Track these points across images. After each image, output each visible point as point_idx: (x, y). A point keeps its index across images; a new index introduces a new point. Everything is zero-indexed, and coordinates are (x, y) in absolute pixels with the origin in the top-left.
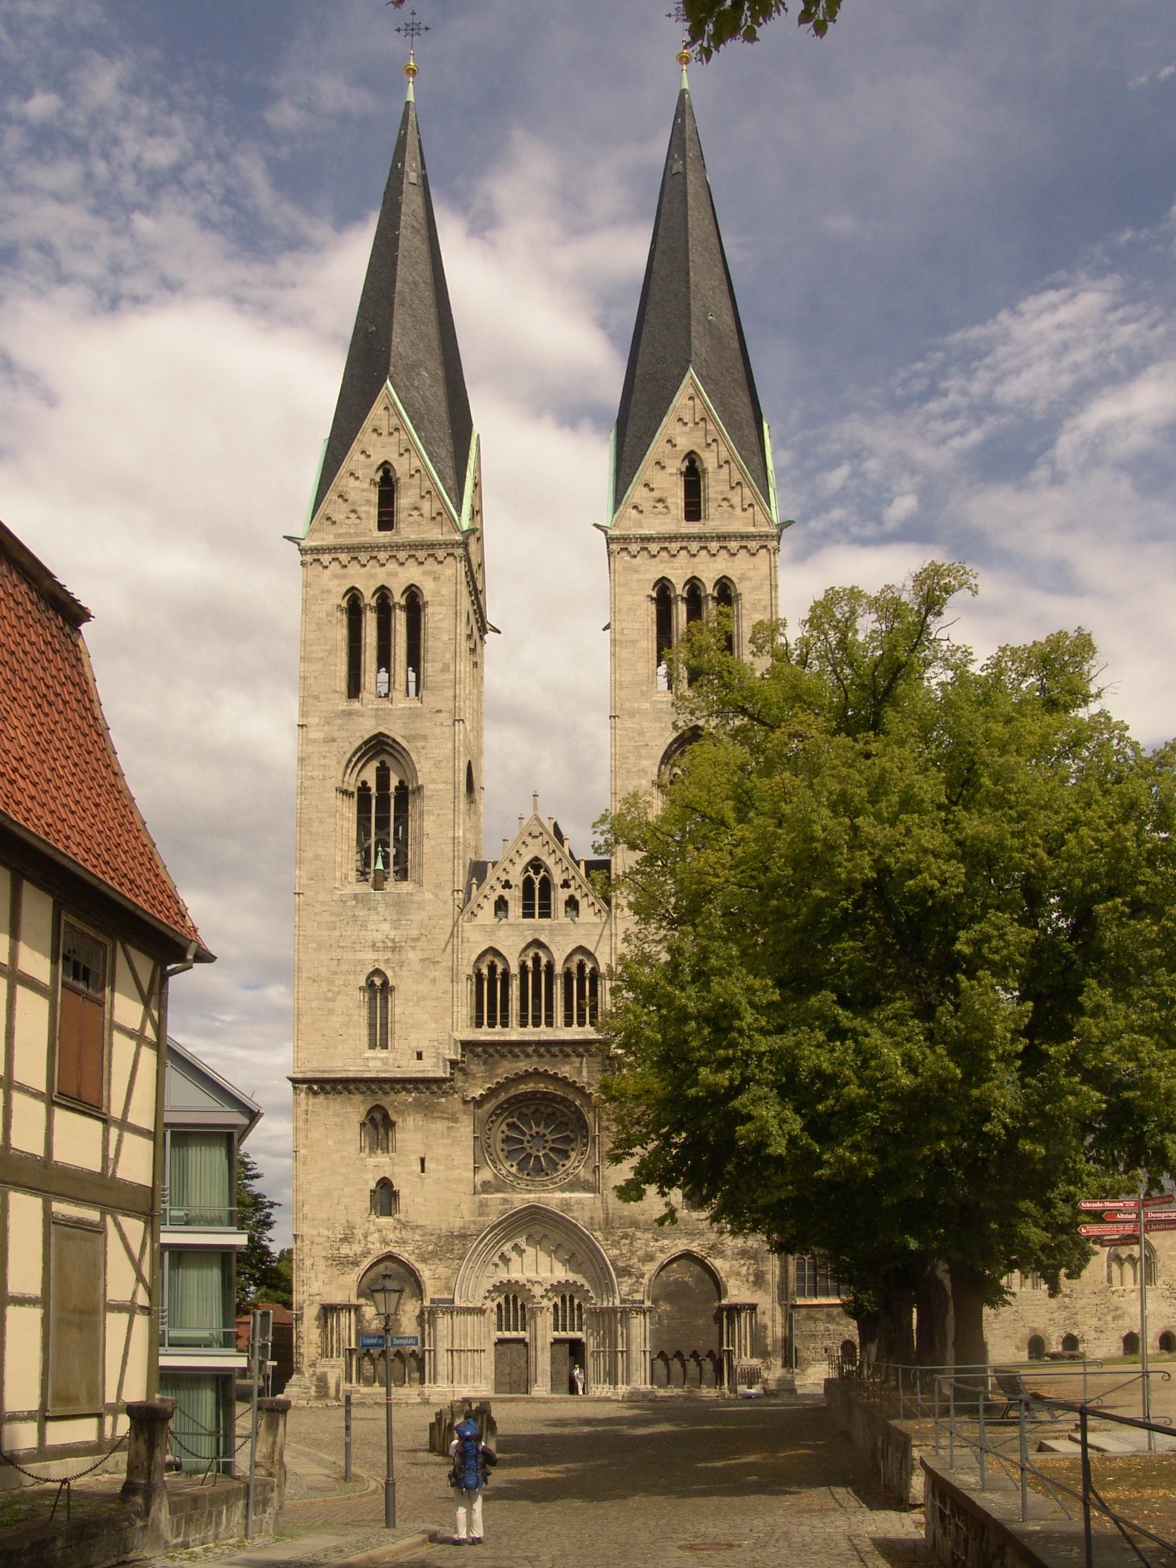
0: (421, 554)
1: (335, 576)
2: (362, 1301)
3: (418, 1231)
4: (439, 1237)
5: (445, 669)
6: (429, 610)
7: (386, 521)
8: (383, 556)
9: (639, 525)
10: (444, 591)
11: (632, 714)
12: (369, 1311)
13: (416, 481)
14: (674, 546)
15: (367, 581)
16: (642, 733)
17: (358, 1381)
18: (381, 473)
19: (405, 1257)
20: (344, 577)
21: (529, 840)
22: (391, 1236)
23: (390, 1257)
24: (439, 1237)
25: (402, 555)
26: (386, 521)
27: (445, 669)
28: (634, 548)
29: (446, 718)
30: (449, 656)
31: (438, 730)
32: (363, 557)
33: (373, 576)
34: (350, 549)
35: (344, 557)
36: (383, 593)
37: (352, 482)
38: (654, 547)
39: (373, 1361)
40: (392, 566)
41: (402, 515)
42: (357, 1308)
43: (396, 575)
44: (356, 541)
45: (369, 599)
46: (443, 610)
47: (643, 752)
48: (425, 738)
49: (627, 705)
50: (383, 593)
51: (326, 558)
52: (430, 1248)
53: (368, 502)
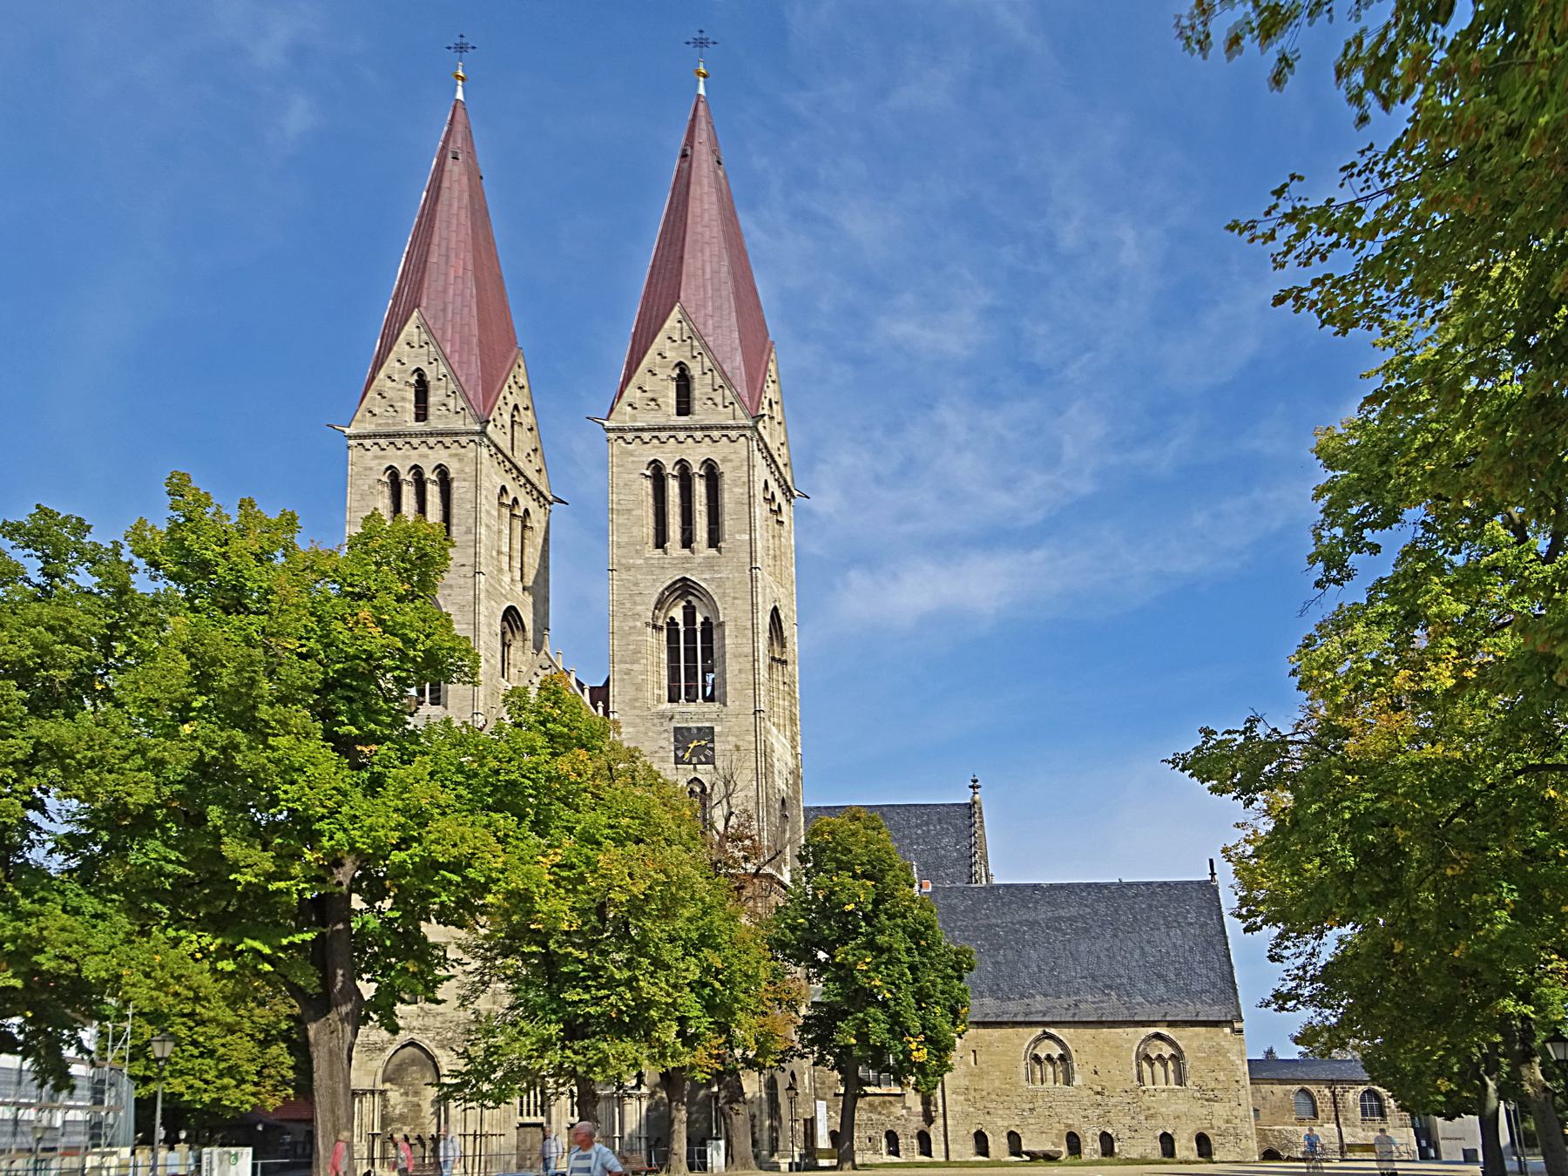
0: (447, 441)
1: (376, 457)
2: (388, 1086)
3: (439, 1018)
4: (458, 1025)
5: (468, 532)
6: (455, 485)
7: (422, 414)
8: (415, 442)
9: (634, 418)
10: (467, 469)
11: (628, 568)
12: (395, 1096)
13: (443, 383)
14: (663, 435)
15: (404, 462)
16: (636, 584)
17: (382, 1165)
18: (415, 377)
19: (426, 1043)
20: (383, 457)
21: (540, 672)
22: (414, 1023)
23: (412, 1043)
24: (458, 1025)
25: (432, 441)
26: (422, 414)
27: (468, 532)
28: (629, 436)
29: (469, 571)
30: (471, 521)
31: (462, 581)
32: (399, 442)
33: (408, 457)
34: (387, 436)
35: (383, 442)
36: (417, 470)
37: (389, 383)
38: (646, 436)
39: (396, 1145)
40: (423, 449)
41: (431, 410)
42: (383, 1093)
43: (426, 456)
44: (392, 429)
45: (406, 476)
46: (466, 484)
47: (637, 599)
48: (451, 587)
49: (623, 561)
50: (417, 470)
51: (368, 443)
52: (449, 1035)
53: (403, 399)
